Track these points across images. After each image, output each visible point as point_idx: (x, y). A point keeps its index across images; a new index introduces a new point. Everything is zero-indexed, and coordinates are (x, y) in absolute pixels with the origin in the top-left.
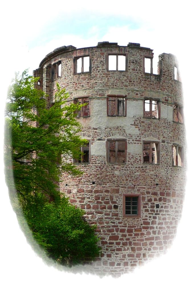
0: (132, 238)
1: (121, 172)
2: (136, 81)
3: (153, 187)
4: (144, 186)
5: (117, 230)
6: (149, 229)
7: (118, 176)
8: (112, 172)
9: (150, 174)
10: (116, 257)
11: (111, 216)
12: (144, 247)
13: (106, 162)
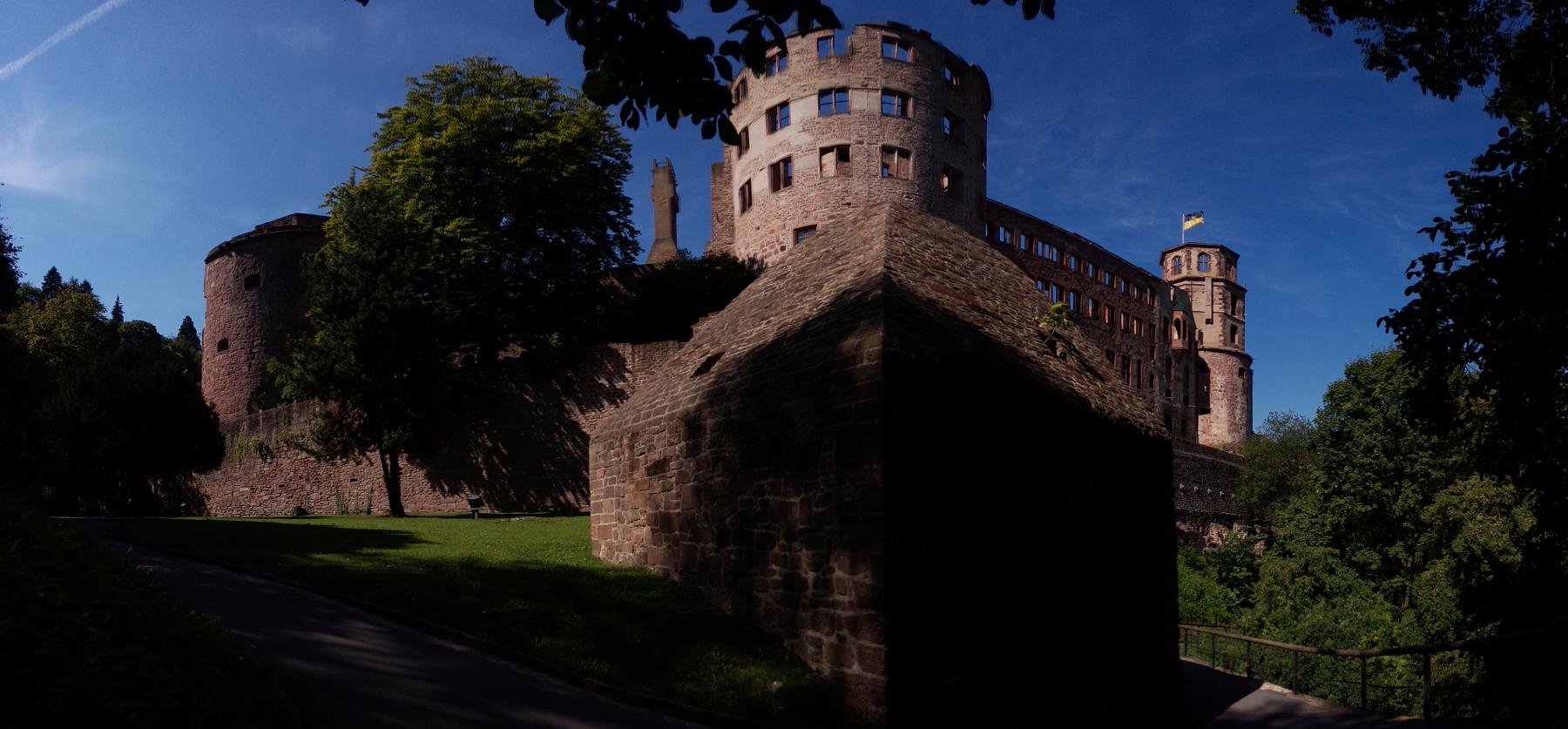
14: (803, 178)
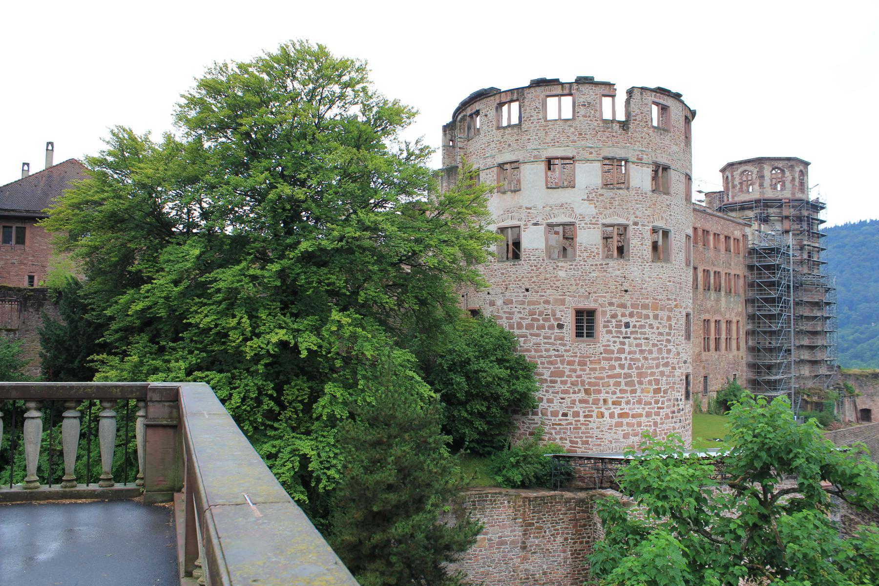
0: (586, 374)
5: (562, 362)
6: (613, 362)
10: (560, 403)
11: (552, 341)
14: (585, 254)
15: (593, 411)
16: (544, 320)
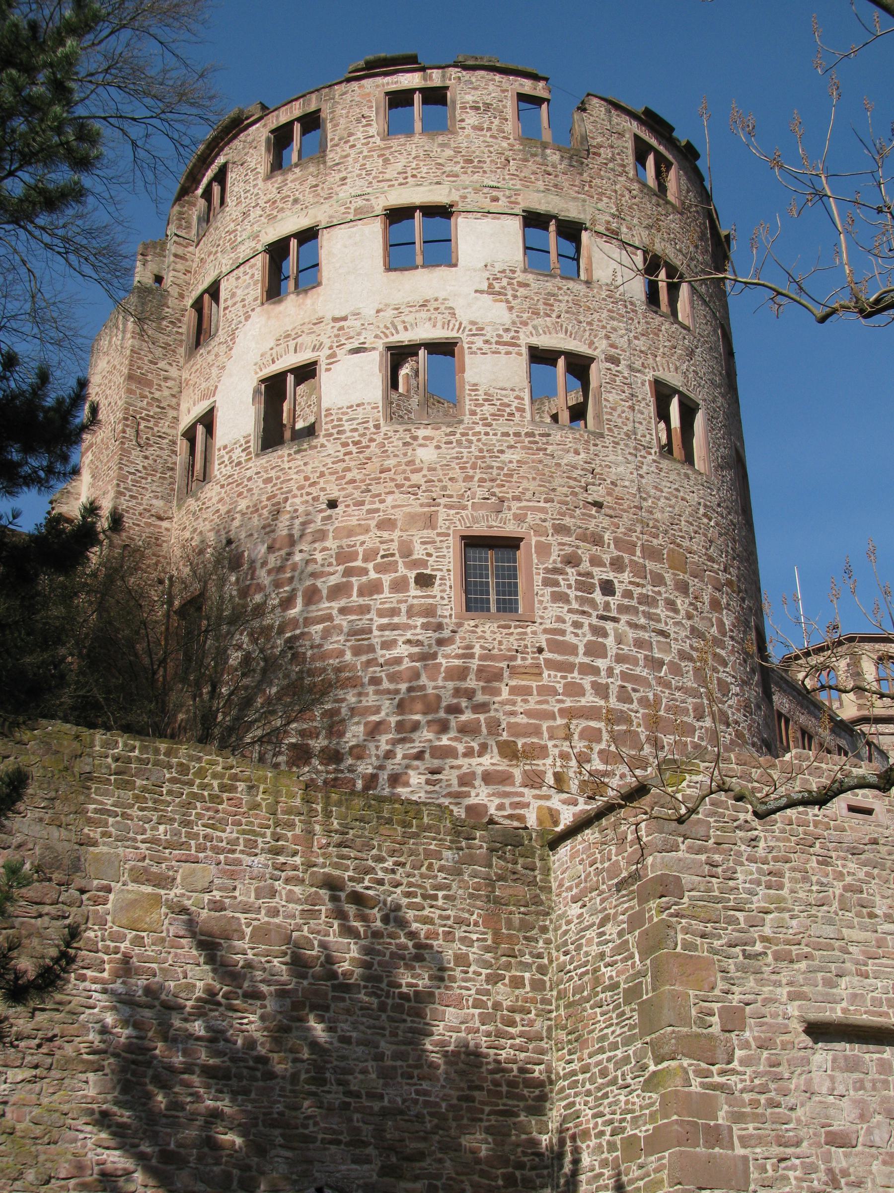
1: (443, 451)
2: (488, 160)
3: (583, 514)
4: (542, 504)
6: (576, 674)
7: (433, 466)
8: (405, 455)
9: (565, 461)
12: (555, 746)
13: (382, 422)
14: (487, 409)
15: (527, 805)
16: (379, 569)
